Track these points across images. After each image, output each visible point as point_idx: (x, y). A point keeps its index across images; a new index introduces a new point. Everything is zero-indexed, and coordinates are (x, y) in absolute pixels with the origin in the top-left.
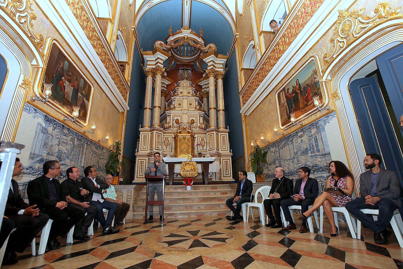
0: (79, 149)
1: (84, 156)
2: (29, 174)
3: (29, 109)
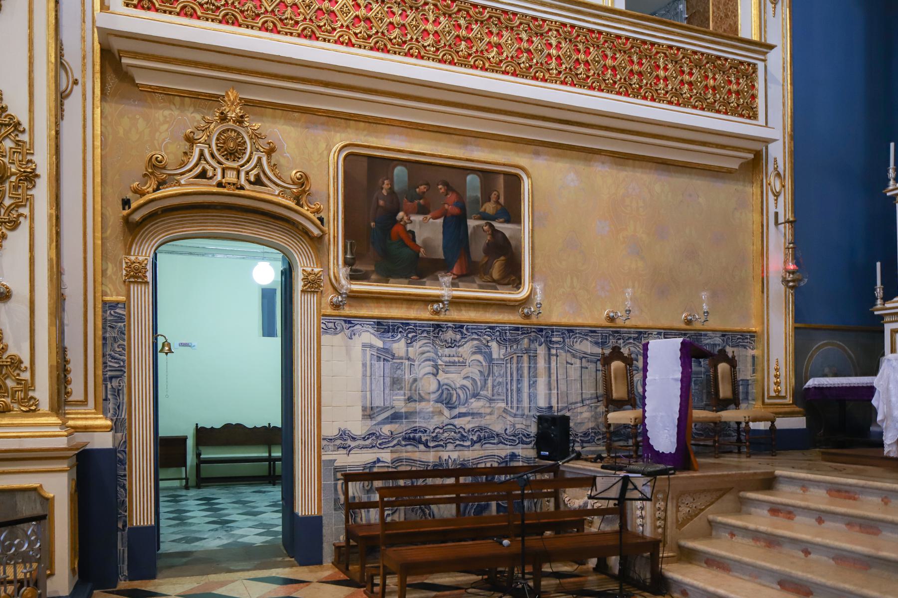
0: (514, 366)
1: (542, 382)
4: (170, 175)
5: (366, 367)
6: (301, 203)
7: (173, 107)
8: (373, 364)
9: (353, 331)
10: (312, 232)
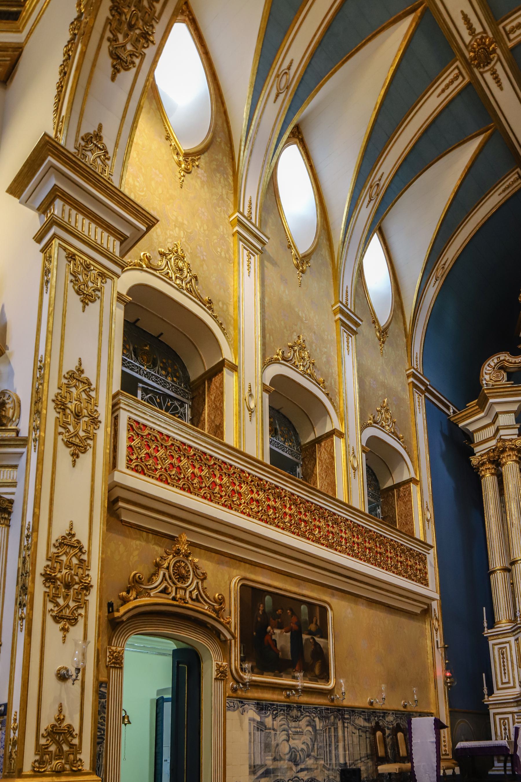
0: (327, 735)
1: (341, 745)
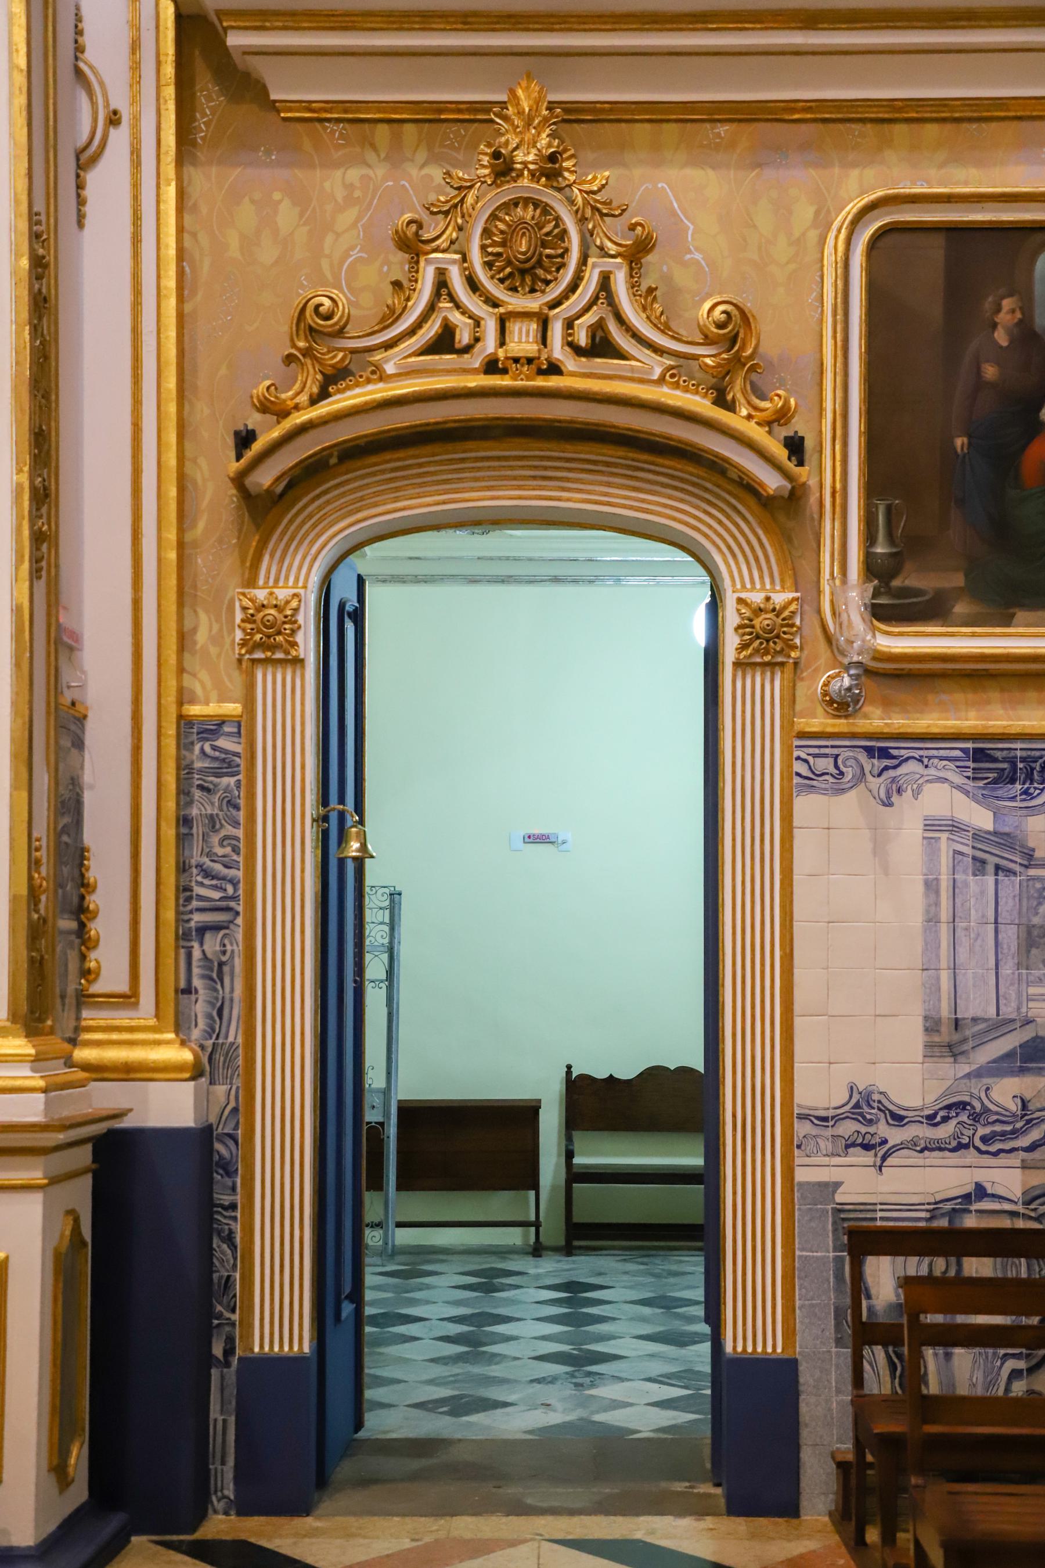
2: (954, 1150)
3: (832, 769)
4: (354, 351)
5: (937, 892)
6: (729, 397)
7: (371, 156)
8: (959, 884)
9: (894, 780)
10: (761, 484)
